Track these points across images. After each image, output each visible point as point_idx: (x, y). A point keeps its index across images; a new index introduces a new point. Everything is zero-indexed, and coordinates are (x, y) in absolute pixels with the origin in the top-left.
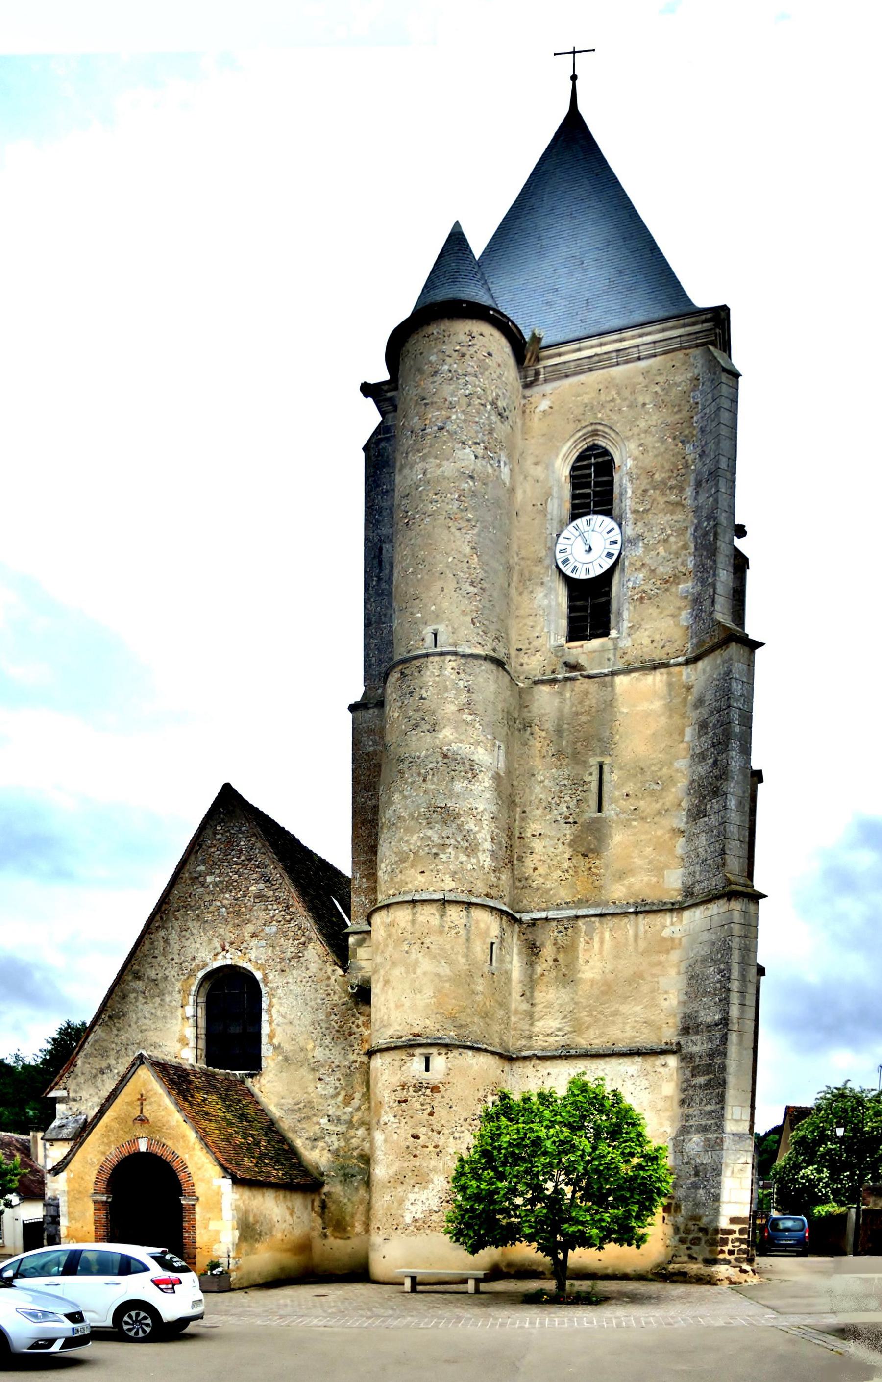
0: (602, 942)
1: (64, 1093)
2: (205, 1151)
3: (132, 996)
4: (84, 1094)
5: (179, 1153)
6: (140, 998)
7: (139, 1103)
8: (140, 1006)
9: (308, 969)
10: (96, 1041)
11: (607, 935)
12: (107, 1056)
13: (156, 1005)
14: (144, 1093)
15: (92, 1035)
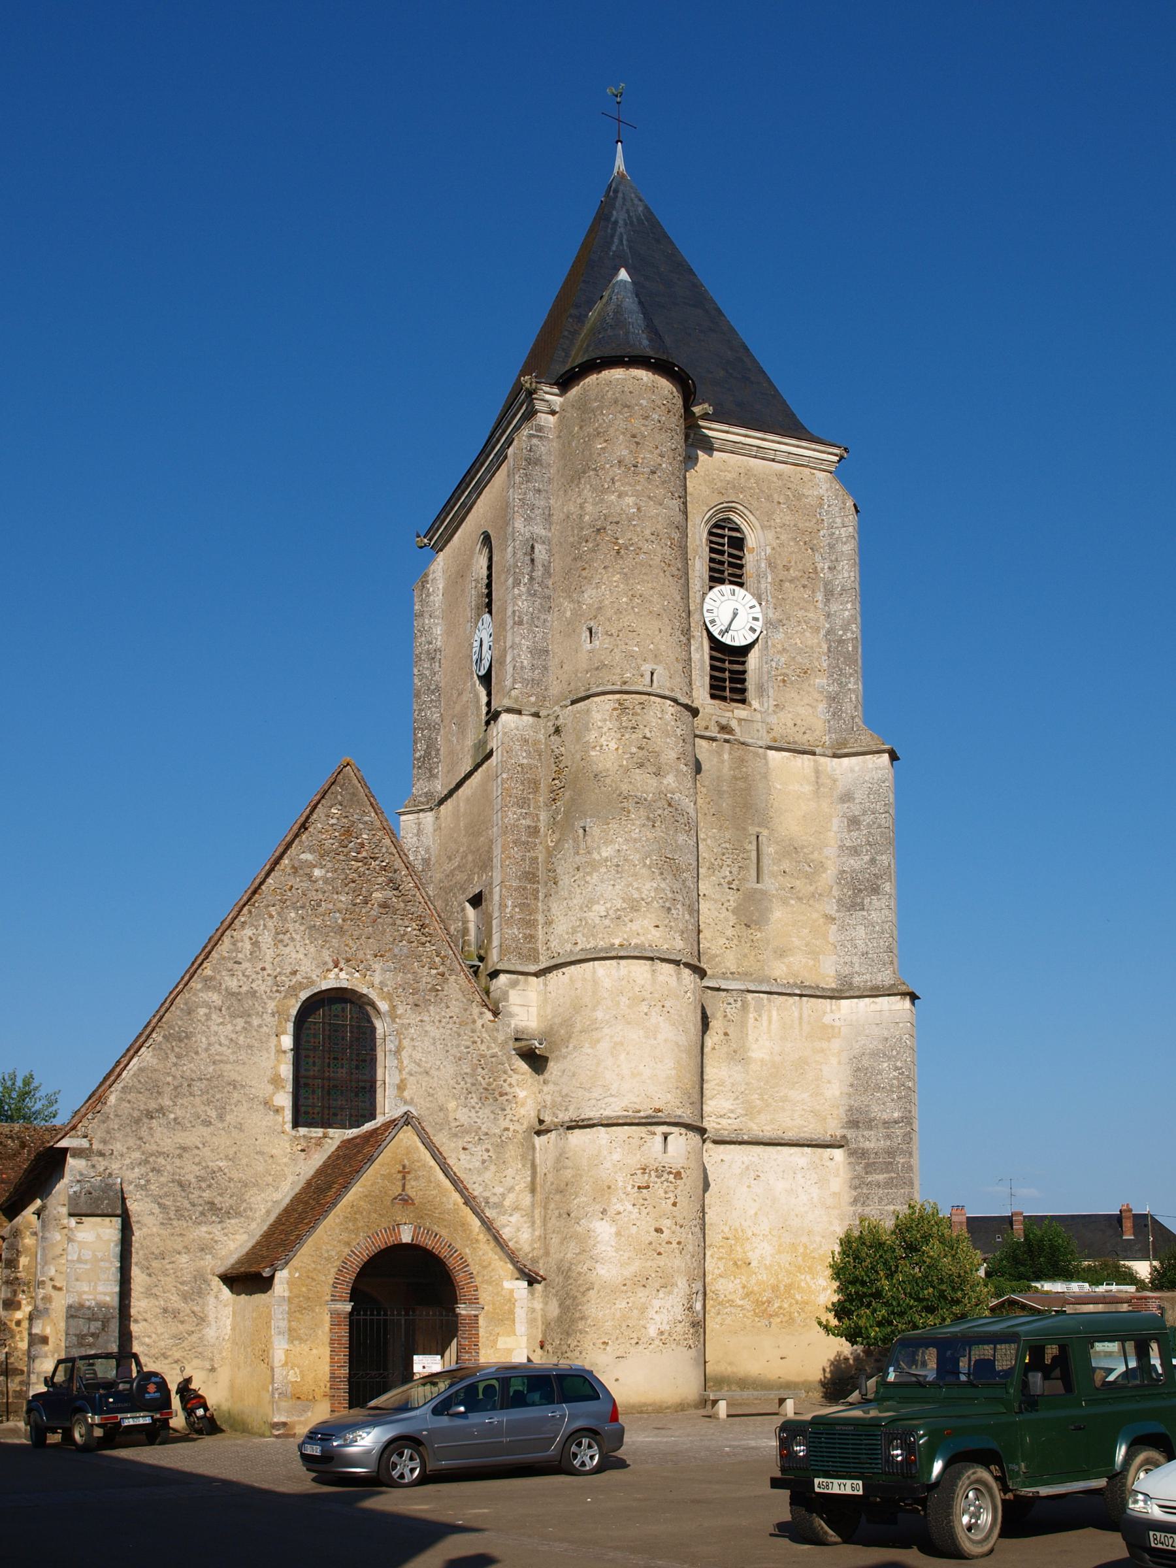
0: (770, 1022)
1: (85, 1143)
2: (493, 1243)
3: (202, 1011)
4: (118, 1147)
5: (458, 1246)
6: (214, 1016)
7: (400, 1176)
8: (214, 1028)
9: (448, 1007)
10: (141, 1070)
11: (774, 1013)
12: (159, 1093)
13: (238, 1028)
14: (406, 1162)
15: (135, 1060)
